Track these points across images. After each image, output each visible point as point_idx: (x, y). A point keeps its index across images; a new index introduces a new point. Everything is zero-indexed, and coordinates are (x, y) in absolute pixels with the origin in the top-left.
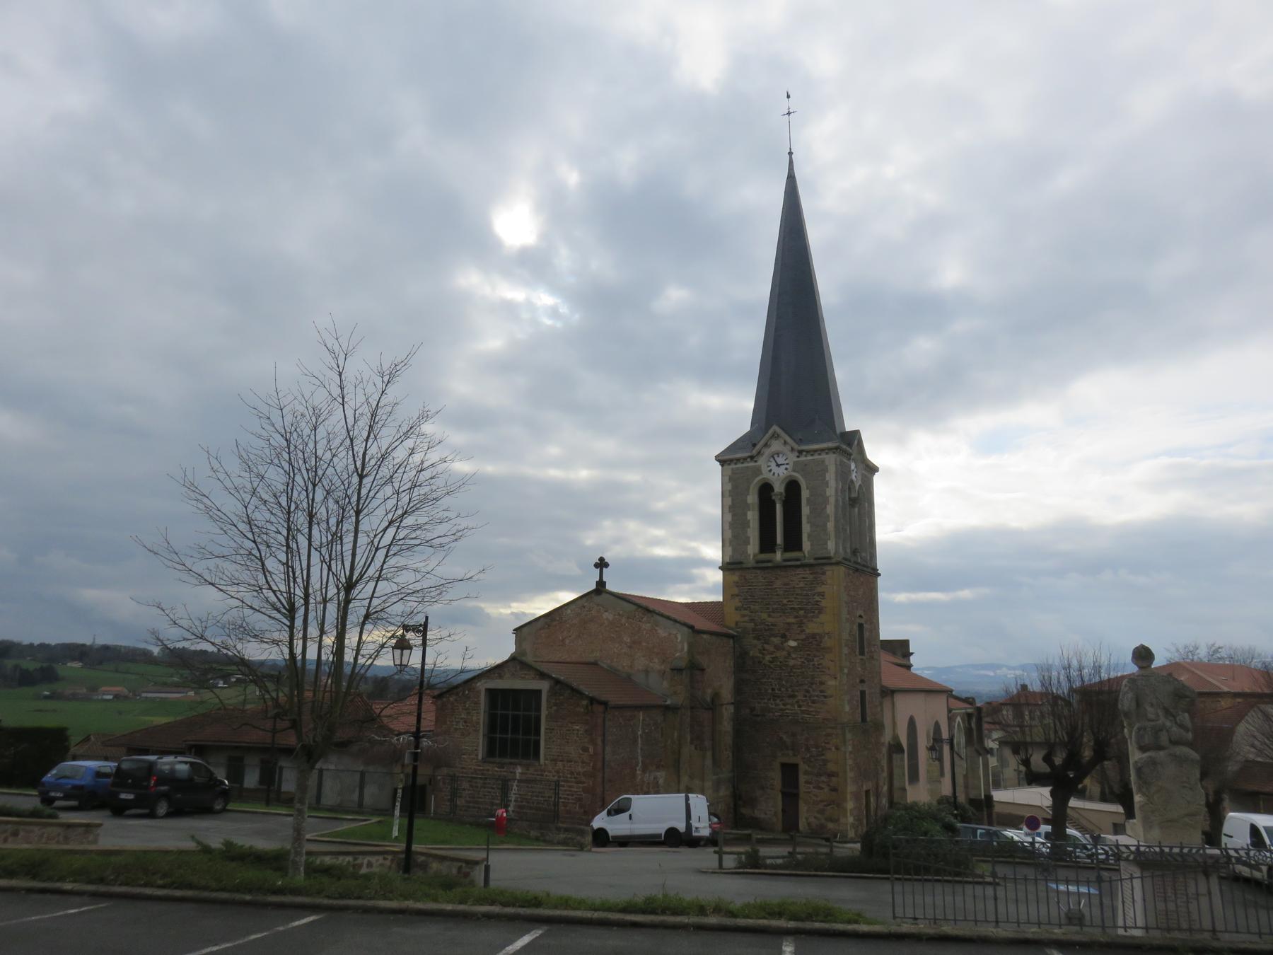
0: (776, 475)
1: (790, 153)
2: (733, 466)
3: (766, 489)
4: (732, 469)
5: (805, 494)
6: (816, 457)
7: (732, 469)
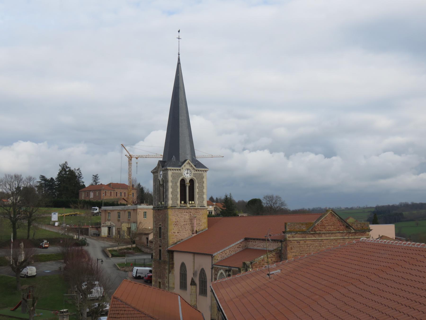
0: (186, 177)
1: (179, 54)
2: (172, 171)
3: (183, 181)
4: (172, 173)
5: (196, 185)
6: (200, 173)
7: (172, 173)
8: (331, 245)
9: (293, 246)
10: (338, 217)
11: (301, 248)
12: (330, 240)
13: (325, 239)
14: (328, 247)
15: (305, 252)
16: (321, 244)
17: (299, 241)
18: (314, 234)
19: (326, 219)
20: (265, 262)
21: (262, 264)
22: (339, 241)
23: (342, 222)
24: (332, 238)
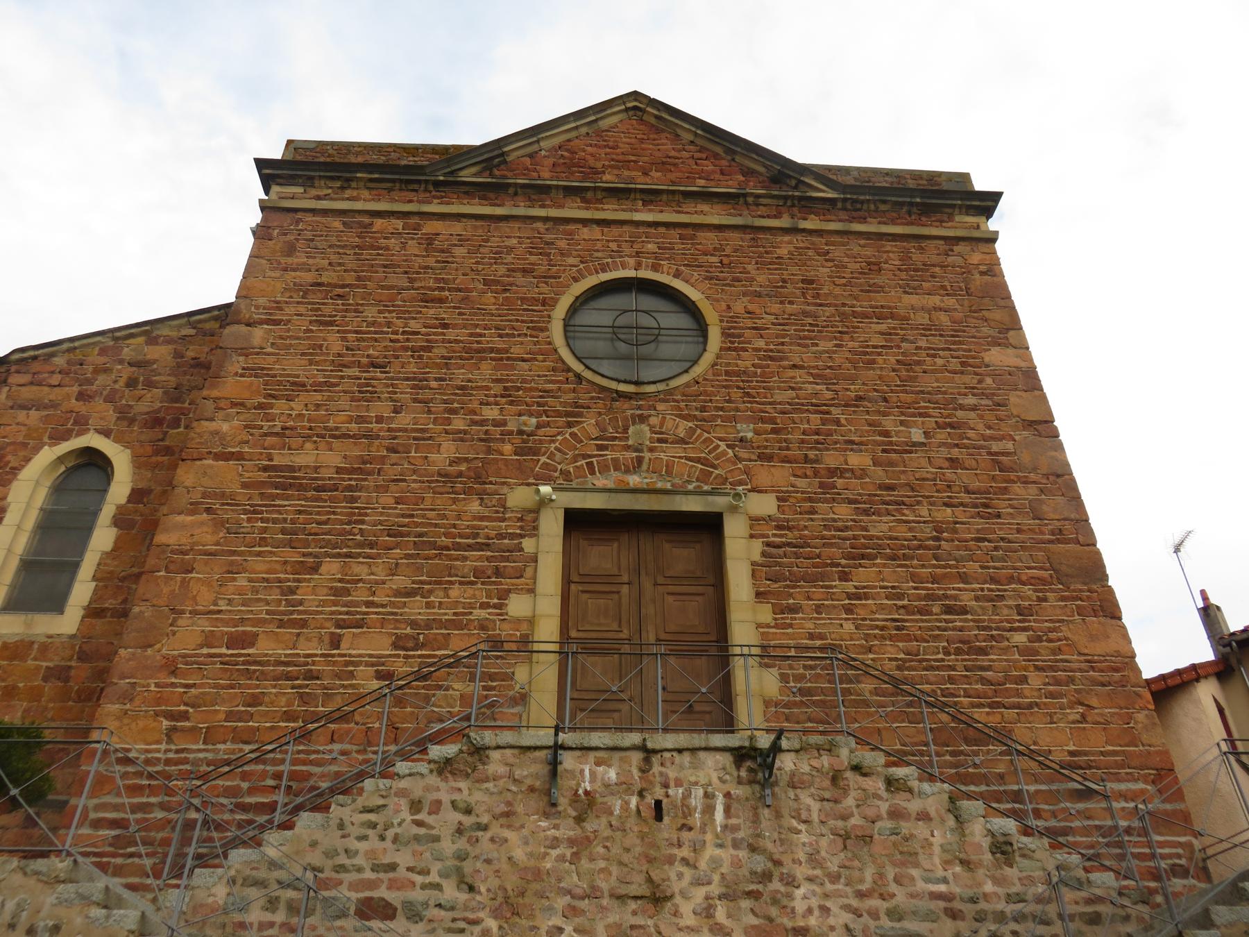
8: (637, 253)
9: (312, 240)
10: (694, 129)
11: (371, 254)
12: (626, 228)
13: (585, 222)
14: (610, 260)
15: (406, 273)
16: (547, 243)
17: (366, 220)
18: (492, 195)
19: (605, 141)
20: (121, 362)
21: (91, 368)
22: (709, 239)
23: (735, 152)
24: (638, 217)
